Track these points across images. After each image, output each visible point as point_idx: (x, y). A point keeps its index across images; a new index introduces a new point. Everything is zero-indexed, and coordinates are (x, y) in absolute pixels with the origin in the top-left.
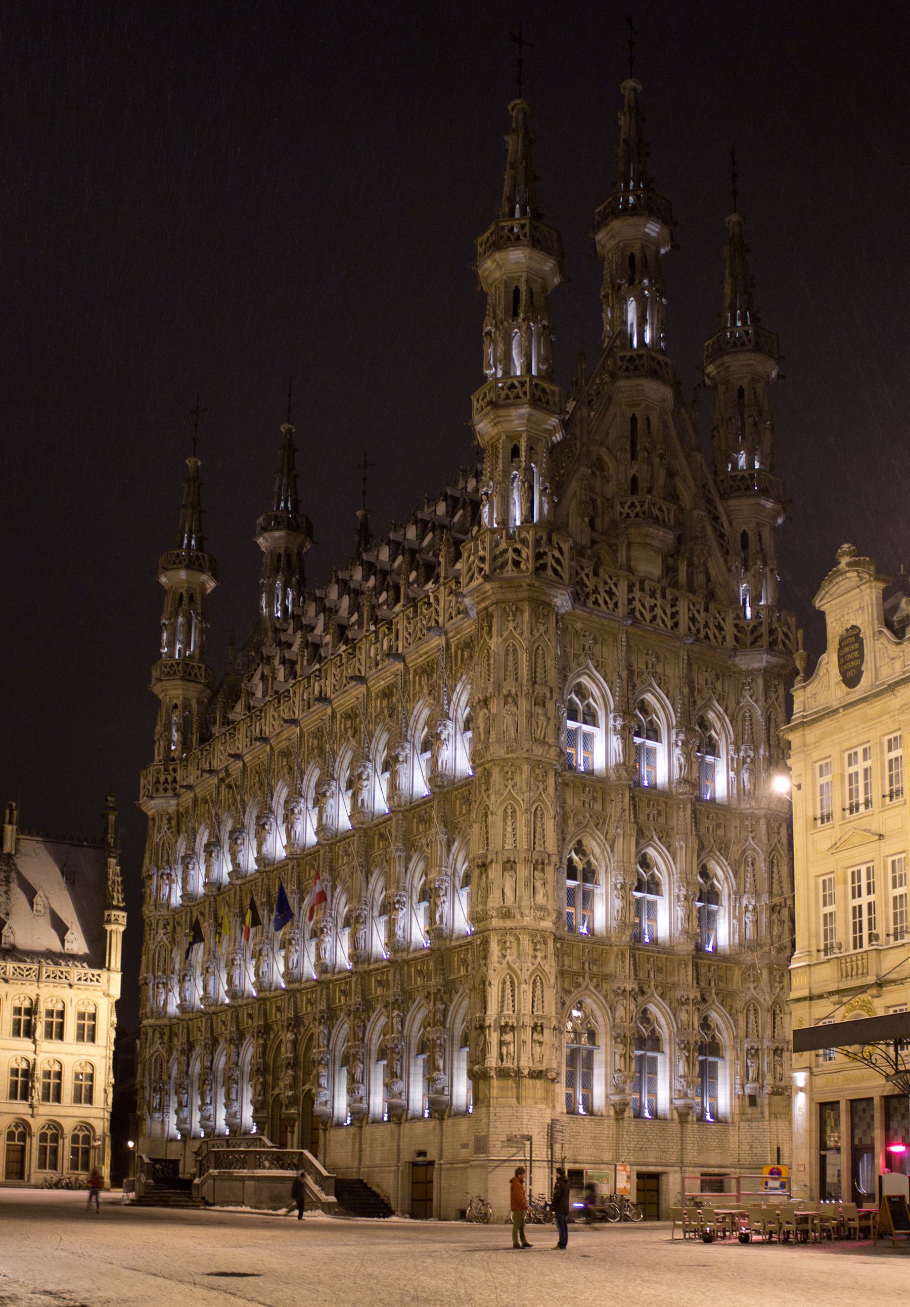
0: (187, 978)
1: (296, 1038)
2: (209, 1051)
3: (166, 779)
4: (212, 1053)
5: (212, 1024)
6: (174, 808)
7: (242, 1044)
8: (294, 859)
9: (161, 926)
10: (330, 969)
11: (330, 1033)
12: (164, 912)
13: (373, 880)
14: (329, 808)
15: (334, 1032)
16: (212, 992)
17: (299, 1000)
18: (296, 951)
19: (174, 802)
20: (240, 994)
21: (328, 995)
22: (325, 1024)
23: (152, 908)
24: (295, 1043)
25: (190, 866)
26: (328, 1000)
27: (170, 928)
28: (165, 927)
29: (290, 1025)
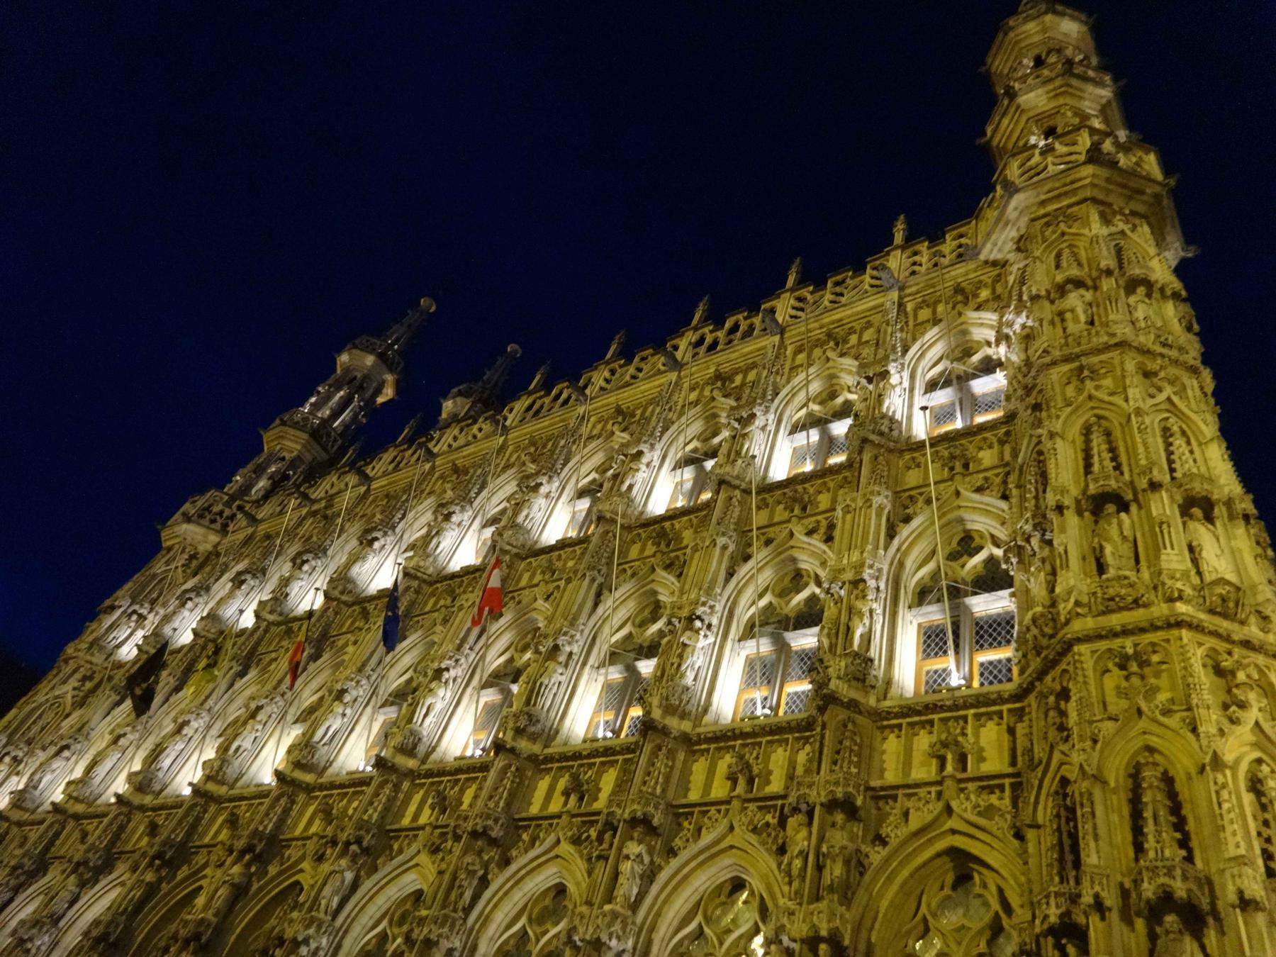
0: (66, 753)
1: (249, 884)
2: (13, 883)
3: (221, 513)
4: (17, 890)
5: (57, 835)
6: (209, 547)
7: (96, 882)
8: (416, 578)
9: (78, 676)
10: (421, 749)
11: (355, 886)
12: (98, 659)
13: (608, 602)
14: (535, 508)
15: (367, 885)
16: (98, 779)
17: (296, 808)
18: (344, 715)
19: (214, 538)
20: (157, 787)
21: (391, 800)
22: (354, 859)
23: (84, 646)
24: (239, 892)
25: (190, 605)
26: (387, 809)
27: (89, 685)
28: (84, 679)
29: (249, 848)
